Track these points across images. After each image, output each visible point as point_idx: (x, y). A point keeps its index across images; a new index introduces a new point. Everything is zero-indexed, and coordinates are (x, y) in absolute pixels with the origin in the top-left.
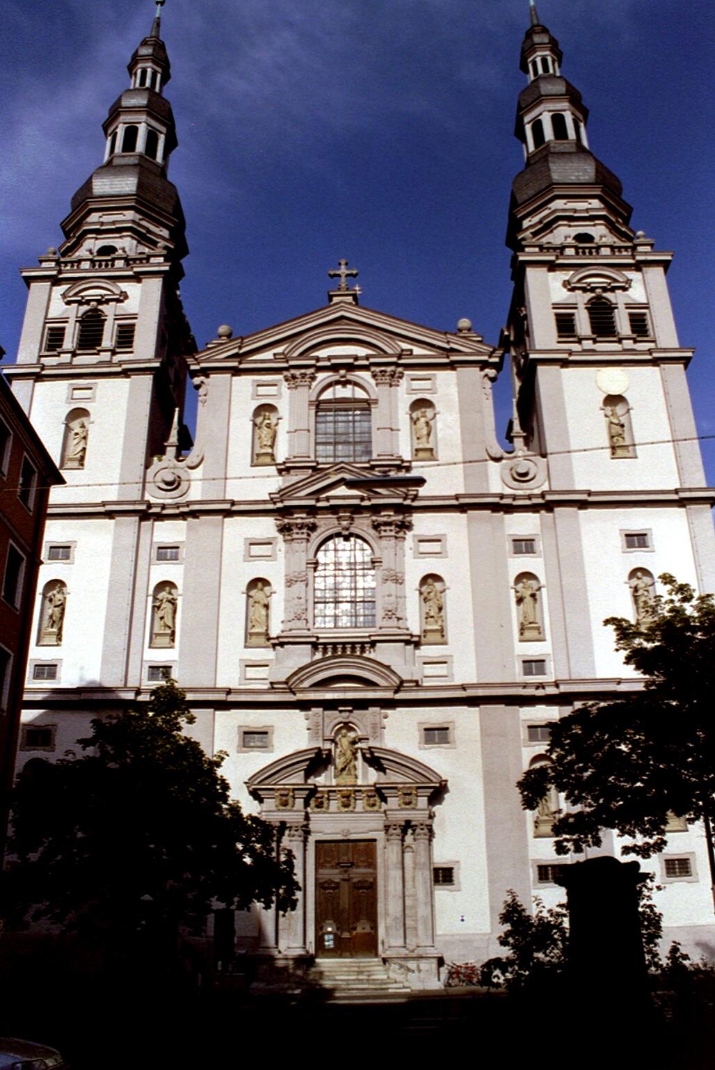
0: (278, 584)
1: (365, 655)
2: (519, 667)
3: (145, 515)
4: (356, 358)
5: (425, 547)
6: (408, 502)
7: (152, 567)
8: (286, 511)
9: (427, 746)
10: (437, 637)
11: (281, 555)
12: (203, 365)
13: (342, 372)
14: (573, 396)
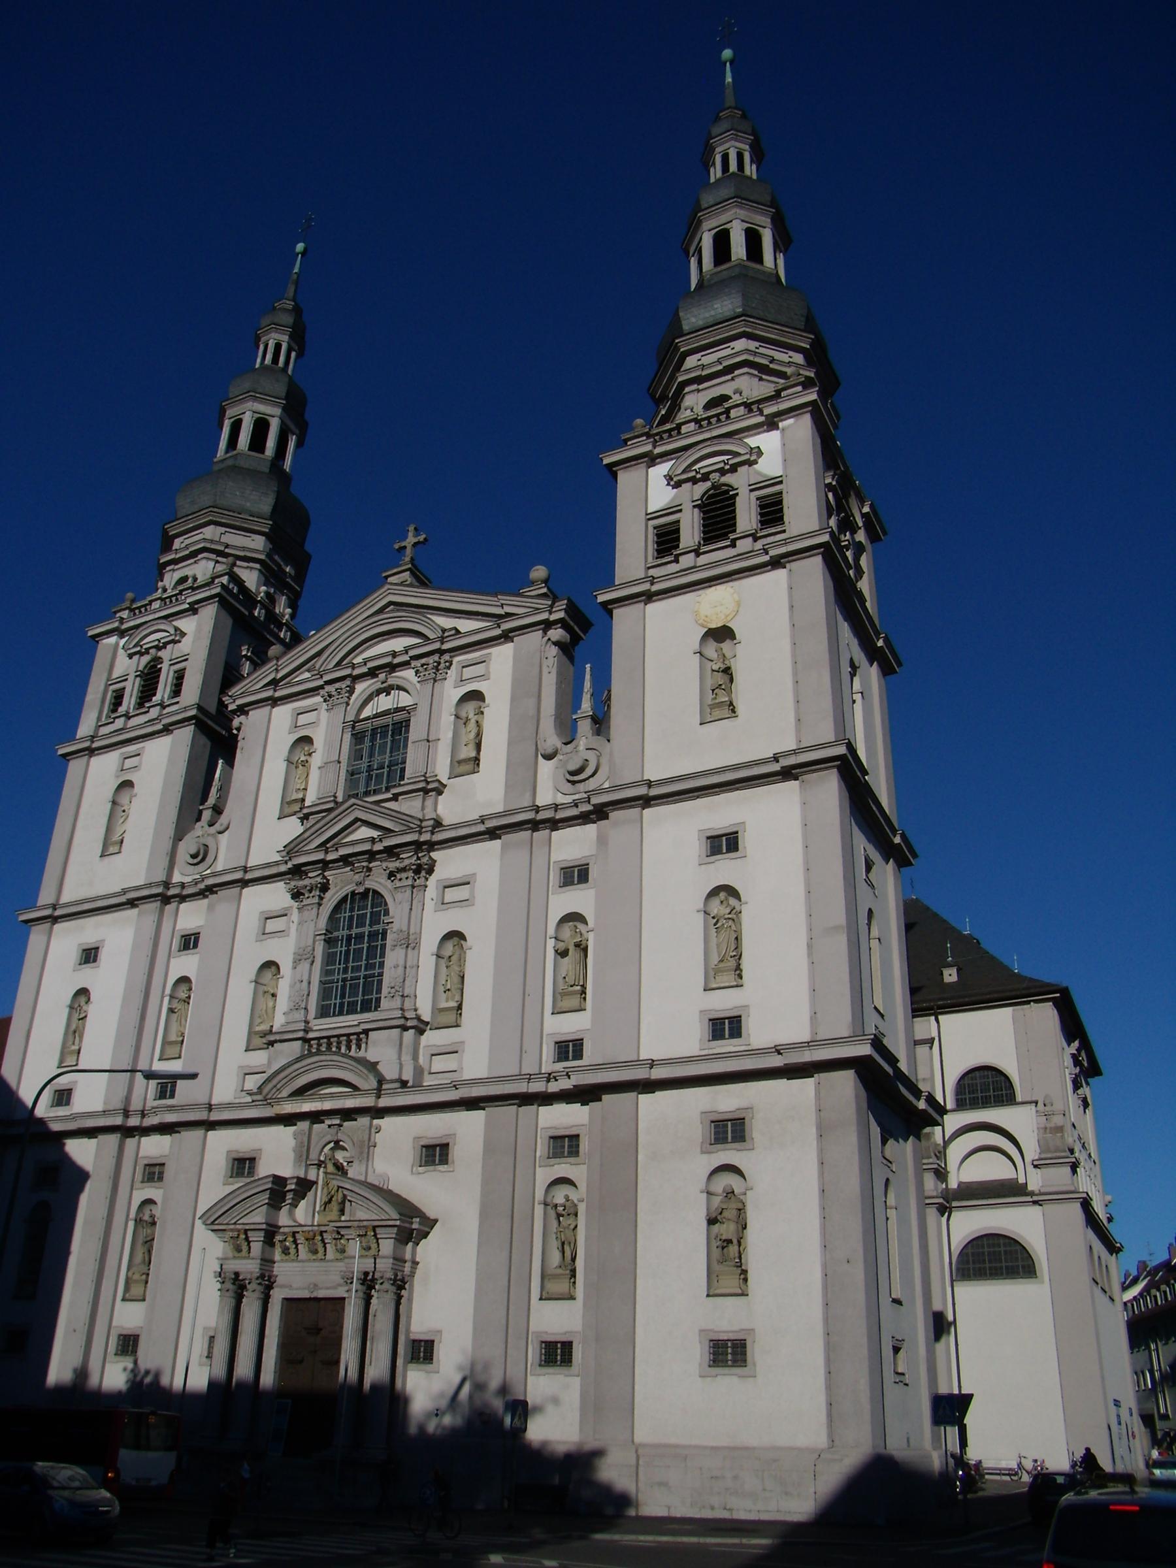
1: (352, 1053)
2: (548, 1051)
3: (166, 900)
4: (394, 654)
5: (451, 895)
6: (425, 837)
7: (172, 960)
8: (298, 871)
9: (421, 1169)
10: (450, 1018)
11: (293, 927)
12: (239, 702)
13: (382, 676)
14: (659, 640)
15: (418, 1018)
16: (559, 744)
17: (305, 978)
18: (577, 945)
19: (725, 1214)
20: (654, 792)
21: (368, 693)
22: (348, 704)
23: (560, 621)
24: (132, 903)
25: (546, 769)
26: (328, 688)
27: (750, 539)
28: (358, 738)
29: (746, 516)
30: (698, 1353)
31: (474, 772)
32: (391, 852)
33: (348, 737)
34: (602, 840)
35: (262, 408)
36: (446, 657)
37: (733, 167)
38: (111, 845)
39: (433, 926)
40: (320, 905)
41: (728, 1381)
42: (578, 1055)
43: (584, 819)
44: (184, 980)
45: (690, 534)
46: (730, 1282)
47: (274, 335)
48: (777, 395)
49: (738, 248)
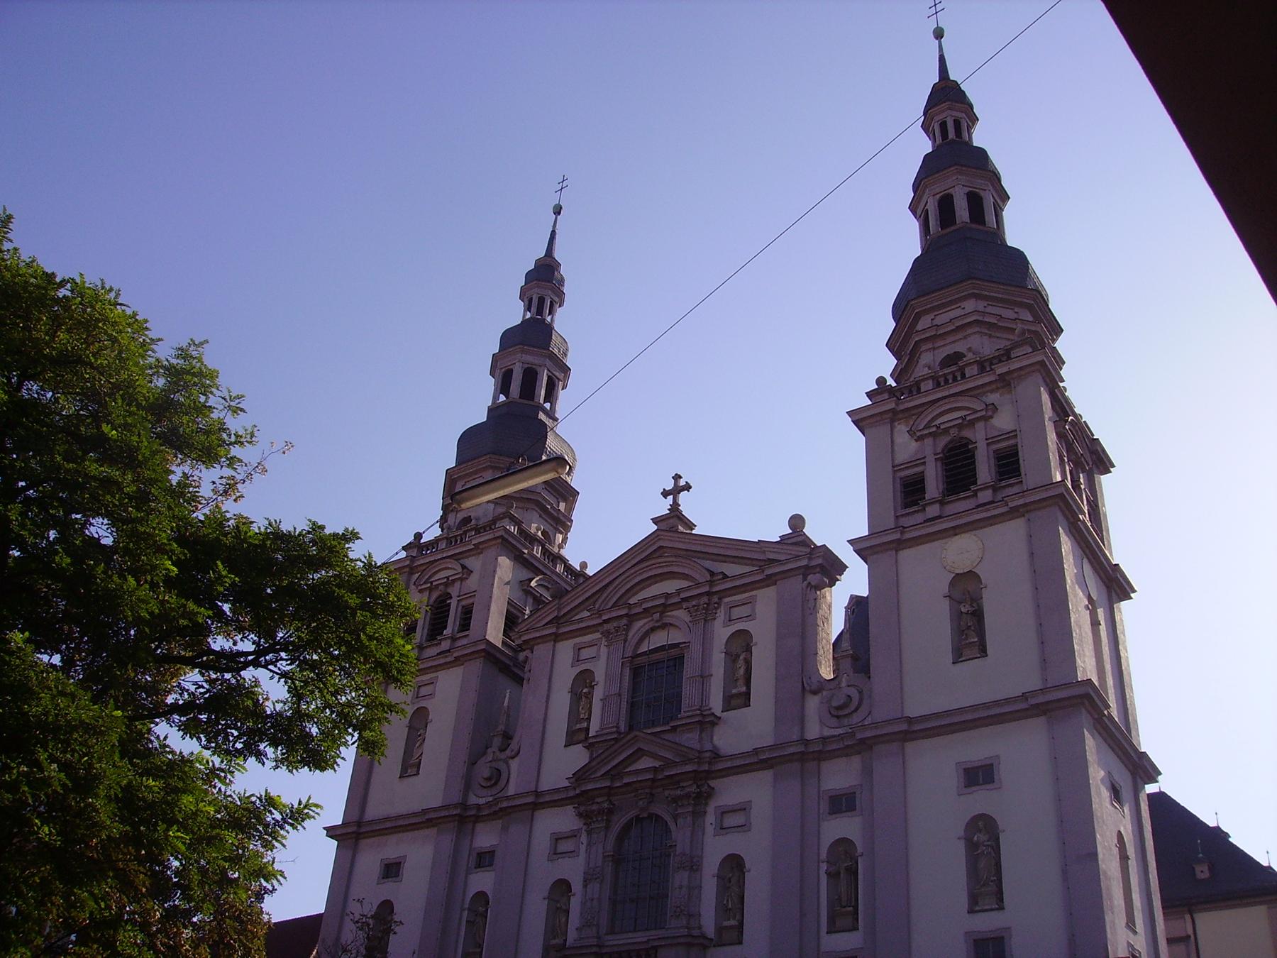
0: (577, 886)
4: (667, 596)
5: (730, 821)
6: (706, 767)
11: (583, 848)
12: (525, 638)
13: (657, 616)
15: (703, 936)
17: (596, 896)
18: (847, 869)
20: (917, 727)
21: (644, 630)
22: (625, 641)
23: (820, 566)
24: (430, 823)
25: (813, 703)
26: (606, 626)
27: (990, 492)
28: (636, 672)
29: (985, 471)
31: (747, 704)
32: (674, 781)
34: (868, 772)
35: (529, 358)
36: (715, 599)
37: (951, 135)
38: (410, 767)
39: (715, 850)
40: (607, 828)
43: (846, 752)
44: (481, 896)
45: (933, 488)
48: (1006, 355)
49: (962, 212)
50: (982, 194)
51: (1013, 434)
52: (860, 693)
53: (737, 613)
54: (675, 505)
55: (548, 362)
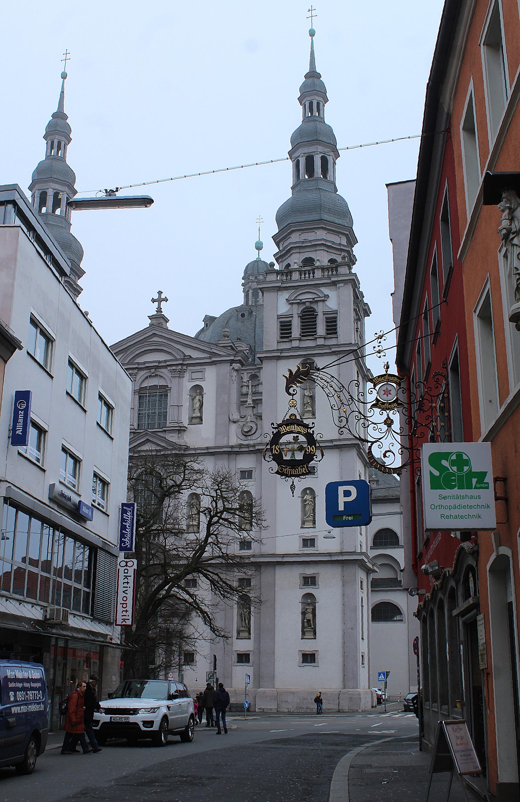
13: (153, 370)
16: (239, 417)
19: (308, 610)
25: (233, 427)
29: (321, 329)
30: (299, 658)
33: (137, 397)
41: (309, 668)
42: (249, 548)
45: (296, 331)
46: (309, 635)
47: (57, 137)
50: (328, 157)
51: (336, 312)
52: (256, 425)
53: (195, 376)
54: (159, 310)
55: (66, 189)
